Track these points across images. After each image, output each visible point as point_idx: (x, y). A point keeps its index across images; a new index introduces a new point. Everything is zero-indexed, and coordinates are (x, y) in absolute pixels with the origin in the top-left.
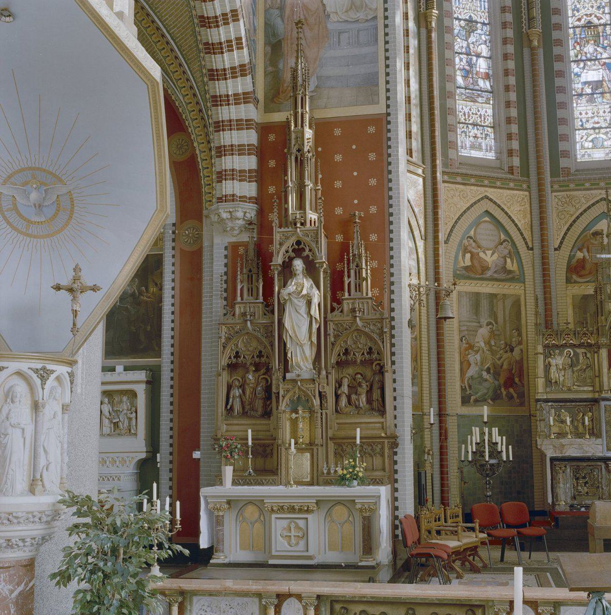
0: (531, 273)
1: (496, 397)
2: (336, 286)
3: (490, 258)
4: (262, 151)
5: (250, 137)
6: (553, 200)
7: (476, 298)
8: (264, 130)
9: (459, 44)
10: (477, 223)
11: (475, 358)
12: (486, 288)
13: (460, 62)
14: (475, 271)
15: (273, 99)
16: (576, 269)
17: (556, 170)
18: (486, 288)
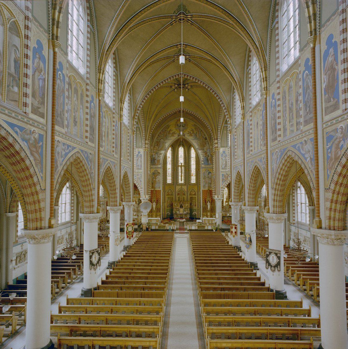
0: (174, 194)
1: (170, 207)
2: (157, 202)
3: (170, 193)
4: (151, 192)
5: (150, 191)
6: (177, 187)
7: (168, 197)
8: (151, 190)
9: (168, 171)
10: (169, 190)
11: (168, 203)
12: (169, 196)
13: (168, 173)
14: (168, 195)
15: (152, 188)
16: (178, 194)
17: (177, 184)
18: (169, 196)
